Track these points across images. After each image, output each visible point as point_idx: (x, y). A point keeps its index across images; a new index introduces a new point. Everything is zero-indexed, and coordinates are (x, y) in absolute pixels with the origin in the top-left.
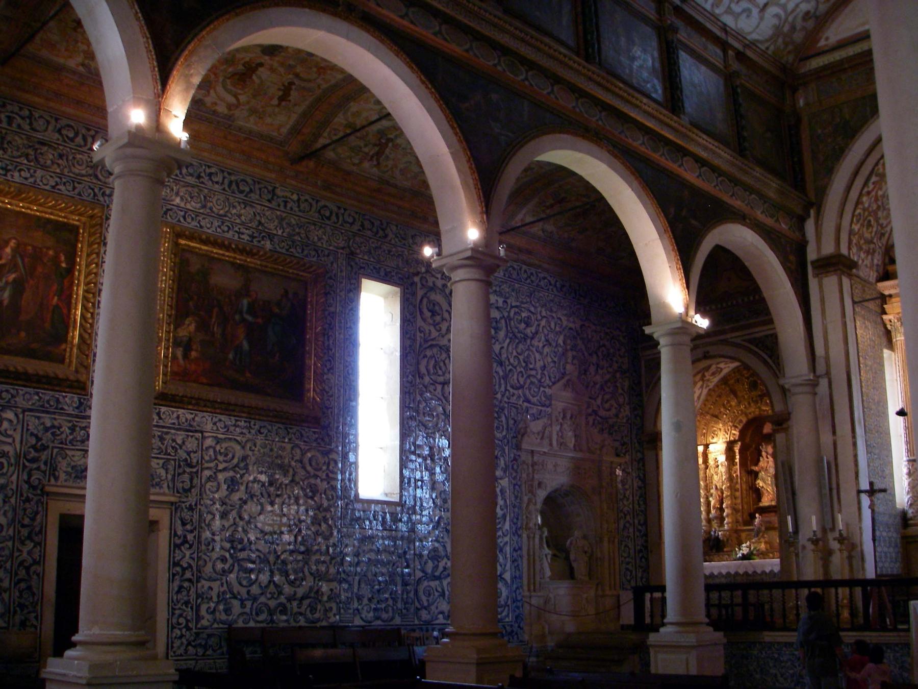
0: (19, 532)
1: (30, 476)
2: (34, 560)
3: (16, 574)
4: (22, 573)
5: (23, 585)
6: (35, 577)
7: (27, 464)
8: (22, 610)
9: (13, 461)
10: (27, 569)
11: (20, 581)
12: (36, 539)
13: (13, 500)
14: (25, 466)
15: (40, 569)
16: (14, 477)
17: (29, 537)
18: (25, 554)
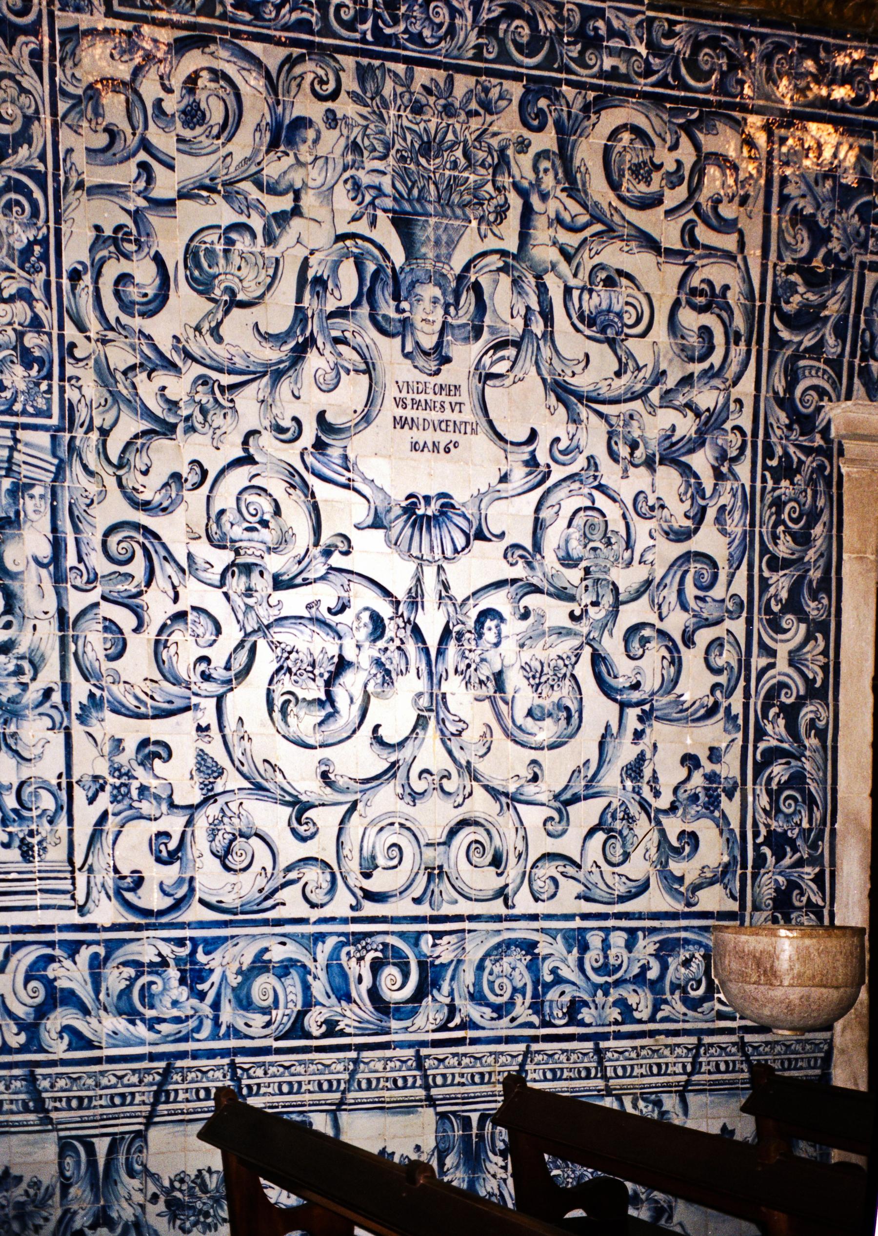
0: (765, 584)
1: (792, 377)
2: (809, 683)
3: (760, 734)
4: (776, 730)
5: (779, 771)
6: (812, 742)
7: (785, 334)
8: (780, 856)
9: (739, 323)
10: (791, 713)
11: (772, 755)
12: (812, 608)
13: (743, 470)
14: (777, 342)
15: (825, 716)
16: (746, 387)
17: (793, 605)
18: (782, 664)
